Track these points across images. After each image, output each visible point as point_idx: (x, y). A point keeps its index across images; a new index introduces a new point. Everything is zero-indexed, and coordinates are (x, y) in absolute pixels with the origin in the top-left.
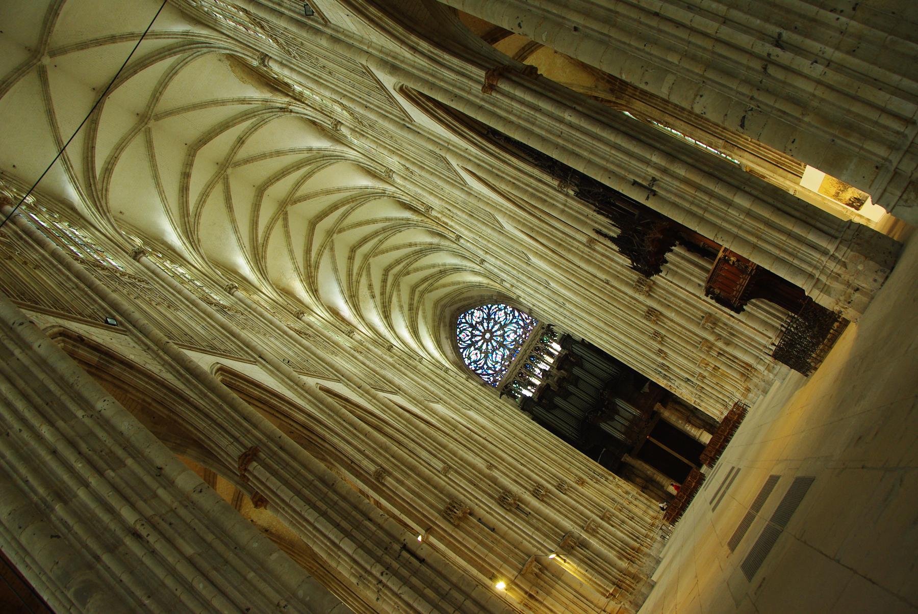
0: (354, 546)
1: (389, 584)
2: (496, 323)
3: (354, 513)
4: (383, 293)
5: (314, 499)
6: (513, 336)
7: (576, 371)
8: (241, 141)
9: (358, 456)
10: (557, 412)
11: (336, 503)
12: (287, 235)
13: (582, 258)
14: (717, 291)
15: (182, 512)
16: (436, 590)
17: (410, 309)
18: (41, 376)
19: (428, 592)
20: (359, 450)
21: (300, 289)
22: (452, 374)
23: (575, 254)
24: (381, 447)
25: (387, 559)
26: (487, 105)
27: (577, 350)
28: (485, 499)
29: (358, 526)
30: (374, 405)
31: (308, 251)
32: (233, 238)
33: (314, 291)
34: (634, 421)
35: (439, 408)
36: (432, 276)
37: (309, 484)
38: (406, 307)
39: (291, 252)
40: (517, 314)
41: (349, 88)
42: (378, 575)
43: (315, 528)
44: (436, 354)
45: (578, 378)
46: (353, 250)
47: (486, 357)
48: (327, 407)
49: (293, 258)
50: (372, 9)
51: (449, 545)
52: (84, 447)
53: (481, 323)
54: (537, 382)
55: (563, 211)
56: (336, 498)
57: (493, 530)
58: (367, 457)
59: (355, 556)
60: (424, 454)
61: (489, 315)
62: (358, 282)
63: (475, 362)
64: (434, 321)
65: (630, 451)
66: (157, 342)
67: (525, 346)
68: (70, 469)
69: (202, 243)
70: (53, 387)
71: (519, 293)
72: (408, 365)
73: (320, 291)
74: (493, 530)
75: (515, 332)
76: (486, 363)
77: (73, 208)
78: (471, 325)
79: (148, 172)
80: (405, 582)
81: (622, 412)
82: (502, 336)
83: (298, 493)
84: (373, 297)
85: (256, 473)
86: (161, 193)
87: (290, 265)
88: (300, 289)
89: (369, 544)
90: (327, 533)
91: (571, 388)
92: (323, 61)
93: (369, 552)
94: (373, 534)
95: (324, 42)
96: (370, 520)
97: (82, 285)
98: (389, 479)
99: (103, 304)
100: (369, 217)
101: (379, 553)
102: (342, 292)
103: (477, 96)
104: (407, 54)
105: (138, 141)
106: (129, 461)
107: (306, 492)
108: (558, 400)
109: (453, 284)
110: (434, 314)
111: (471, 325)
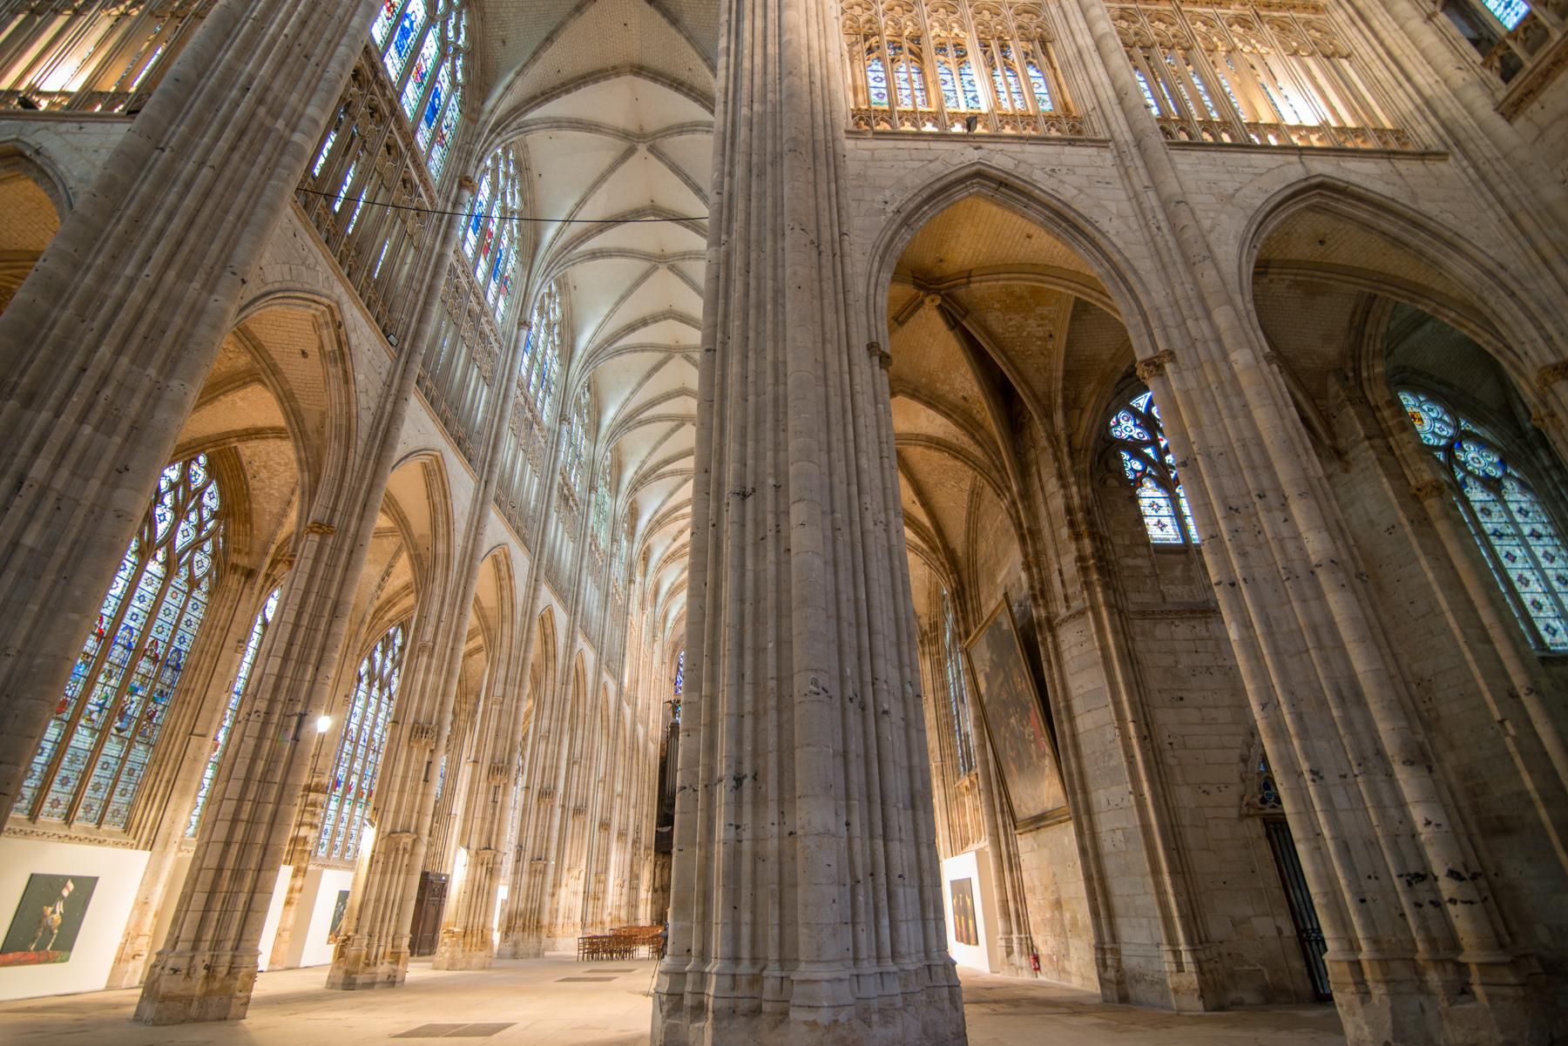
0: (276, 670)
5: (309, 609)
9: (433, 620)
12: (667, 436)
15: (80, 513)
18: (178, 320)
20: (439, 617)
21: (629, 474)
22: (657, 647)
25: (278, 708)
29: (302, 662)
30: (525, 602)
31: (667, 462)
32: (627, 393)
37: (323, 596)
49: (650, 454)
52: (108, 392)
56: (323, 627)
58: (437, 627)
62: (676, 519)
68: (69, 394)
70: (170, 335)
74: (426, 780)
77: (536, 246)
79: (622, 290)
86: (613, 311)
87: (644, 453)
89: (286, 682)
93: (276, 687)
94: (302, 680)
97: (422, 297)
99: (413, 324)
105: (641, 266)
106: (117, 440)
107: (312, 598)
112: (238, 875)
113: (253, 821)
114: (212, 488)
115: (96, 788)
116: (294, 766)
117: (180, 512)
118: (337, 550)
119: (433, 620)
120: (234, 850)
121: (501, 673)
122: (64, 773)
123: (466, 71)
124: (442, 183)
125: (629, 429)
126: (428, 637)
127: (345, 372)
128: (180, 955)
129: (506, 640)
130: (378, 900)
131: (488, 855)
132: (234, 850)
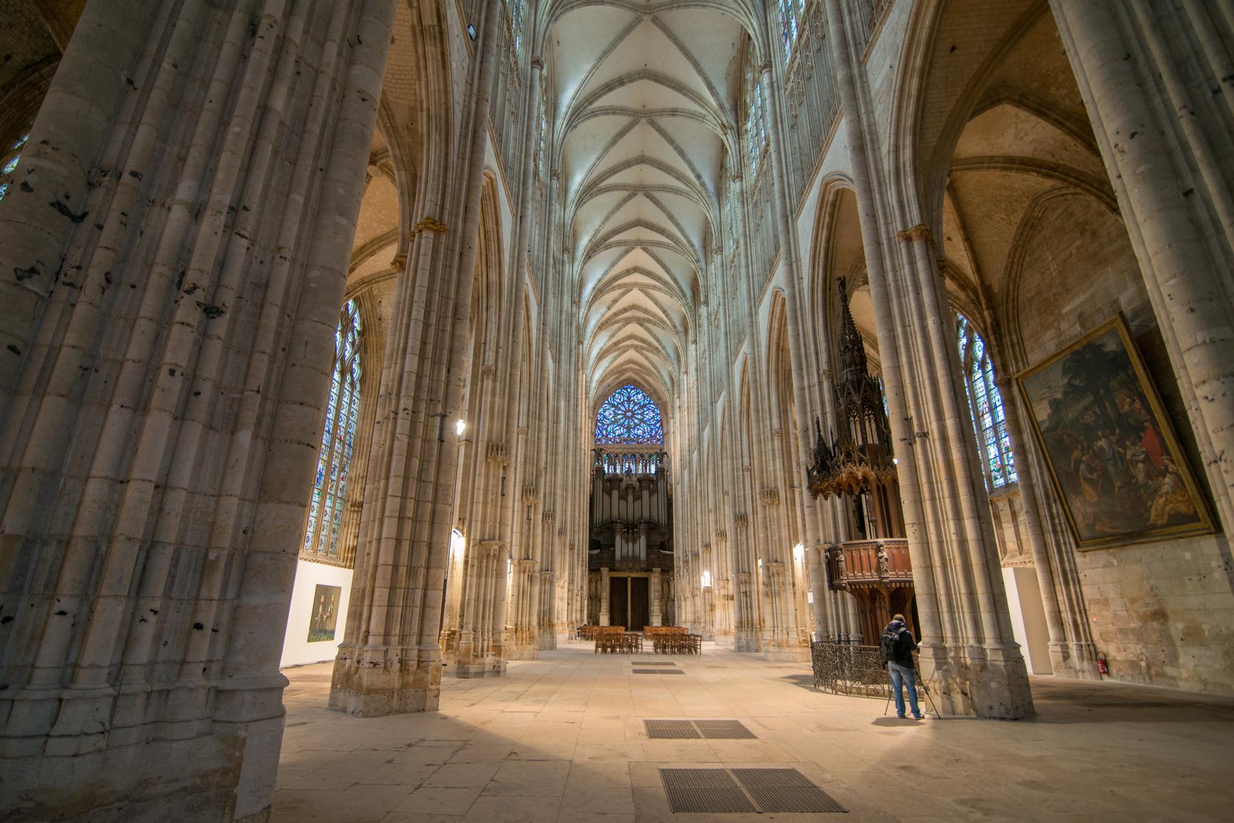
0: (415, 368)
1: (400, 422)
2: (642, 414)
3: (446, 352)
4: (615, 314)
5: (435, 307)
6: (640, 432)
7: (645, 493)
10: (606, 498)
11: (444, 331)
12: (619, 206)
13: (759, 435)
14: (842, 557)
16: (421, 470)
17: (615, 344)
19: (416, 463)
20: (498, 343)
23: (758, 428)
25: (423, 407)
26: (886, 247)
27: (661, 484)
28: (519, 476)
29: (436, 362)
33: (588, 256)
35: (563, 404)
36: (650, 344)
37: (445, 297)
38: (615, 339)
39: (608, 218)
41: (789, 151)
42: (402, 406)
43: (408, 325)
44: (594, 385)
45: (640, 498)
46: (636, 269)
47: (613, 423)
50: (915, 81)
51: (466, 466)
53: (635, 404)
54: (618, 471)
55: (802, 389)
56: (449, 328)
58: (497, 353)
59: (405, 375)
60: (524, 406)
61: (645, 406)
62: (614, 289)
63: (605, 417)
64: (616, 367)
66: (481, 90)
69: (575, 131)
71: (677, 416)
72: (576, 364)
73: (589, 263)
74: (503, 495)
78: (629, 398)
80: (412, 435)
82: (636, 425)
83: (430, 291)
85: (423, 241)
88: (584, 242)
89: (426, 382)
90: (410, 336)
91: (630, 498)
92: (803, 113)
93: (418, 387)
95: (840, 75)
96: (449, 371)
100: (668, 266)
101: (424, 395)
102: (600, 280)
103: (888, 232)
104: (885, 147)
107: (436, 298)
108: (615, 493)
110: (622, 365)
111: (629, 398)
112: (412, 572)
113: (416, 520)
116: (443, 467)
118: (450, 250)
119: (493, 345)
120: (406, 546)
126: (490, 361)
127: (443, 54)
128: (375, 649)
130: (477, 599)
131: (528, 564)
132: (406, 546)
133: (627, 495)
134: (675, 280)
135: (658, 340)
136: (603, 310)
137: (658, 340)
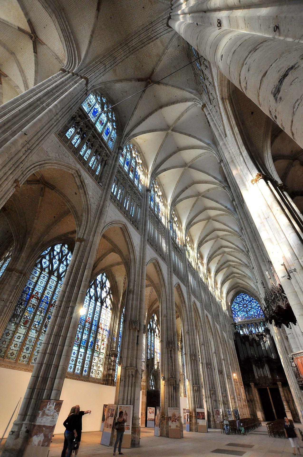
2: (251, 305)
4: (221, 266)
6: (252, 313)
8: (208, 190)
9: (132, 281)
20: (134, 280)
24: (141, 286)
34: (266, 377)
40: (260, 308)
48: (143, 262)
53: (247, 301)
57: (137, 344)
58: (134, 284)
61: (251, 301)
62: (216, 256)
63: (235, 309)
65: (256, 385)
67: (253, 319)
74: (137, 344)
75: (254, 313)
76: (237, 312)
78: (243, 299)
81: (264, 370)
82: (250, 310)
84: (218, 264)
91: (255, 345)
98: (131, 295)
108: (247, 343)
109: (246, 282)
111: (243, 299)
114: (70, 254)
115: (27, 349)
117: (61, 262)
118: (86, 246)
121: (164, 305)
122: (27, 346)
123: (116, 126)
124: (113, 150)
125: (192, 226)
127: (85, 191)
129: (164, 293)
133: (253, 344)
134: (237, 246)
135: (243, 272)
136: (216, 265)
137: (243, 272)
